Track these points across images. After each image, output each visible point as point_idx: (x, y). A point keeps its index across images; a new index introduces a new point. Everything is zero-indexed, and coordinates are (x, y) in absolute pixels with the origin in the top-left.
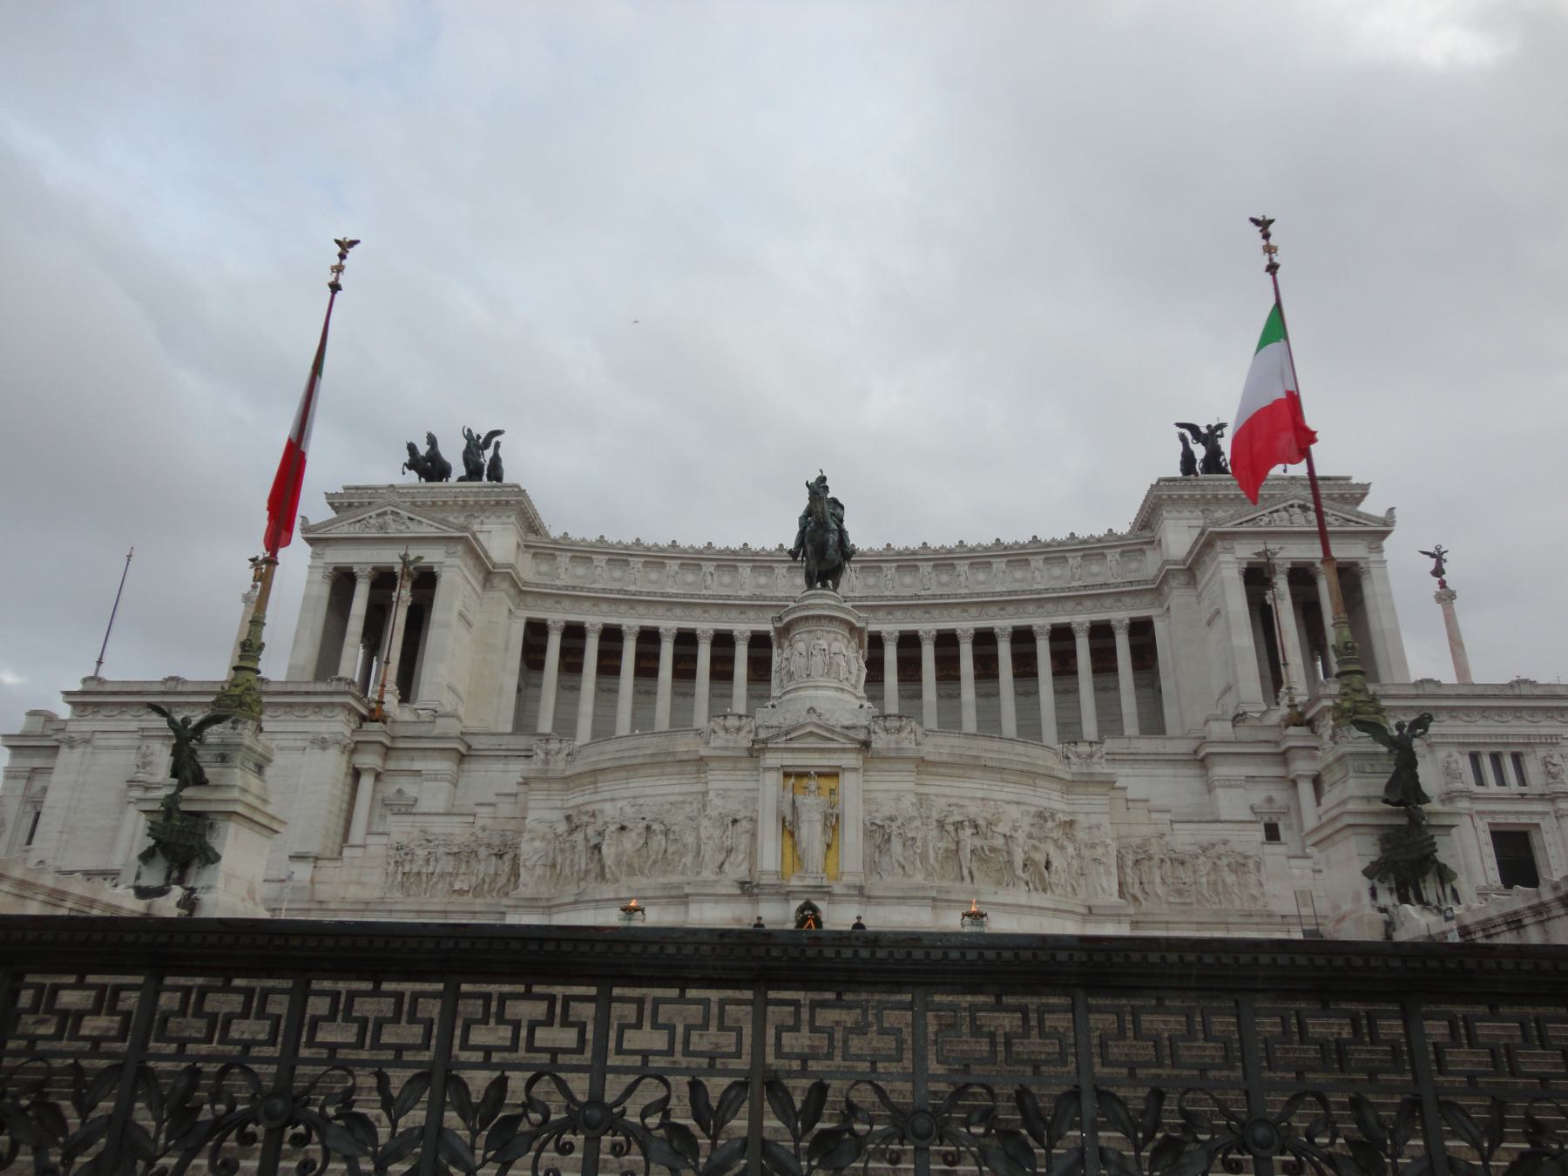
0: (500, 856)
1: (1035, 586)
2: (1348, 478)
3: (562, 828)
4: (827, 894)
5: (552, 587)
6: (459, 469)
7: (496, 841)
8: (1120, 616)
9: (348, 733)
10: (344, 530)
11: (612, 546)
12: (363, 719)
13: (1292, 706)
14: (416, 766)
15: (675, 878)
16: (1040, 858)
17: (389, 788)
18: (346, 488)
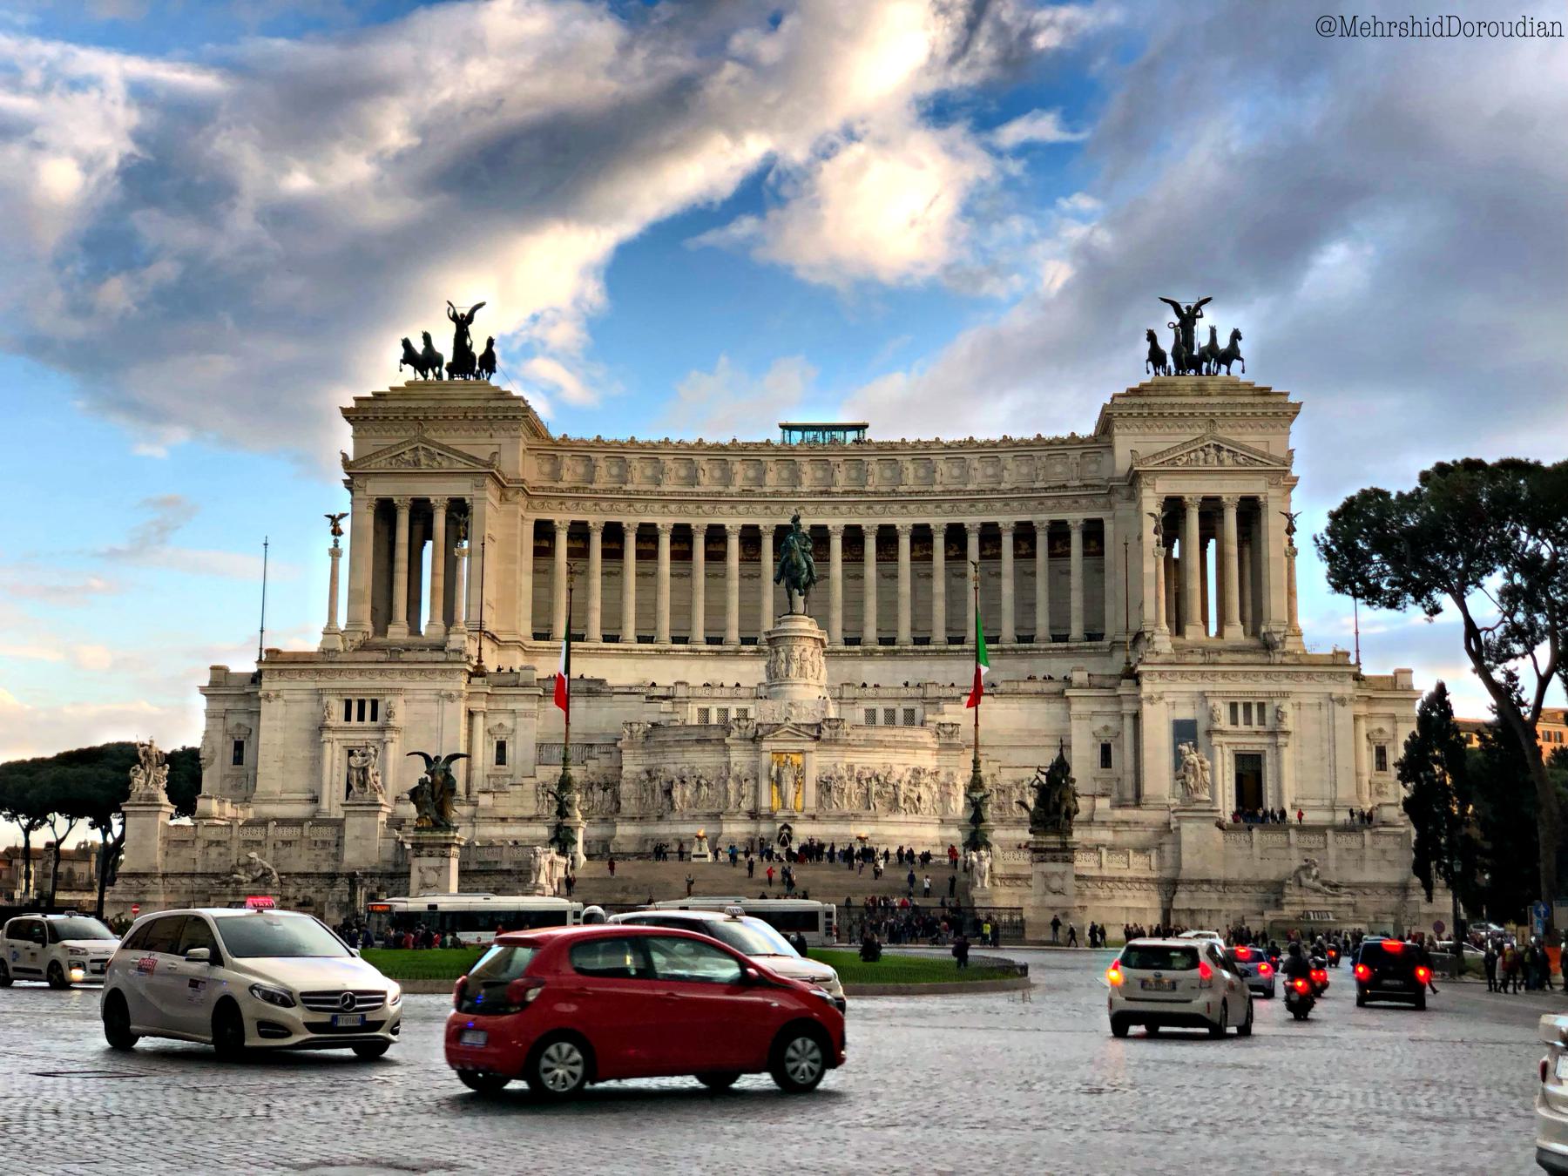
0: (605, 790)
1: (1003, 486)
2: (1287, 394)
3: (644, 777)
4: (793, 818)
5: (557, 490)
6: (448, 357)
7: (602, 781)
8: (1076, 518)
9: (463, 687)
10: (382, 464)
11: (608, 445)
12: (471, 675)
13: (1128, 663)
14: (511, 706)
15: (715, 810)
16: (915, 796)
17: (494, 721)
18: (357, 399)
